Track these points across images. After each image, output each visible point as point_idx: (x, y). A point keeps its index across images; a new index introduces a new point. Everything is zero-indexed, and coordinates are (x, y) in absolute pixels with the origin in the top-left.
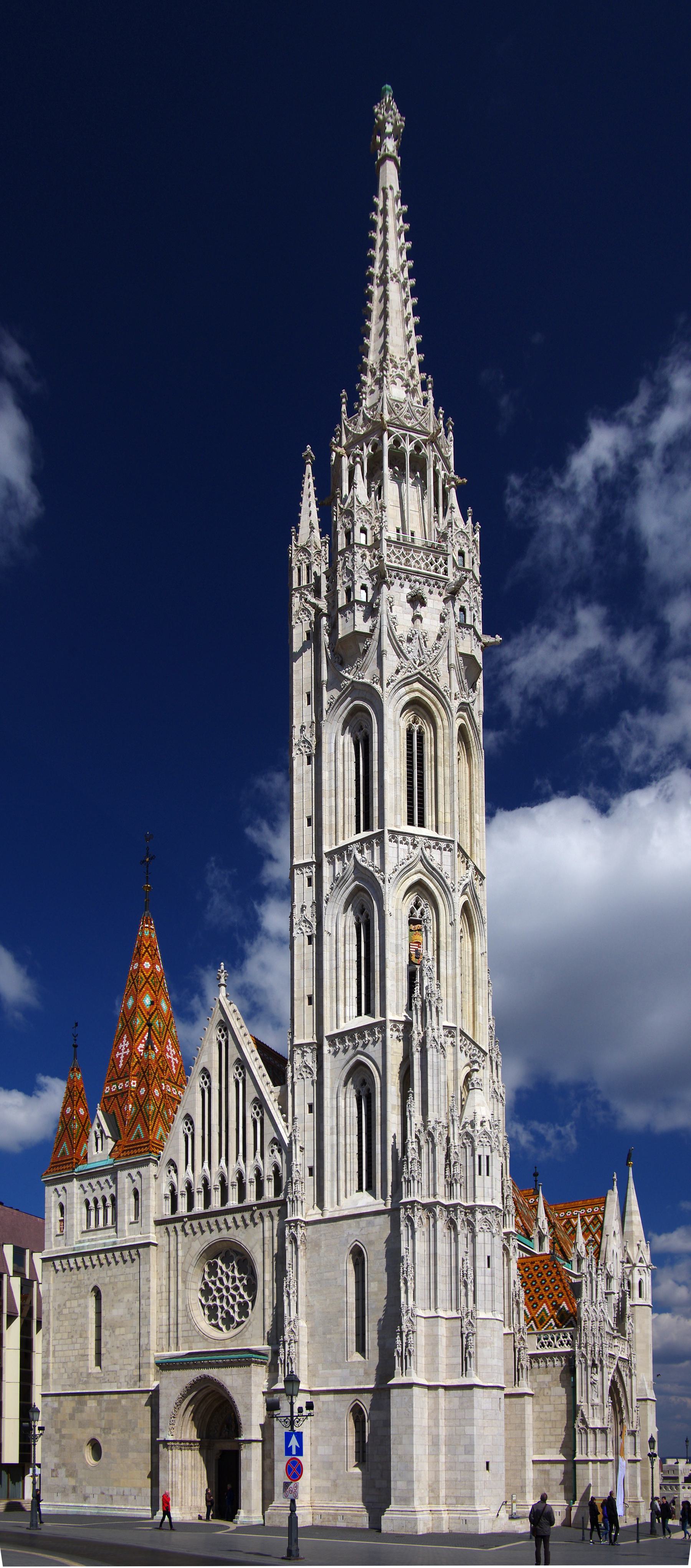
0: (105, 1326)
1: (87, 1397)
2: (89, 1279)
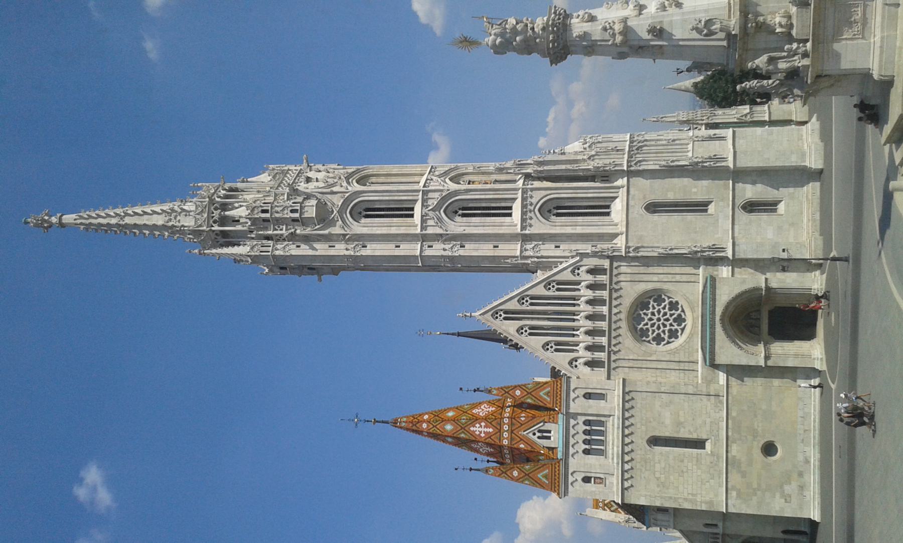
1: (729, 454)
2: (641, 449)
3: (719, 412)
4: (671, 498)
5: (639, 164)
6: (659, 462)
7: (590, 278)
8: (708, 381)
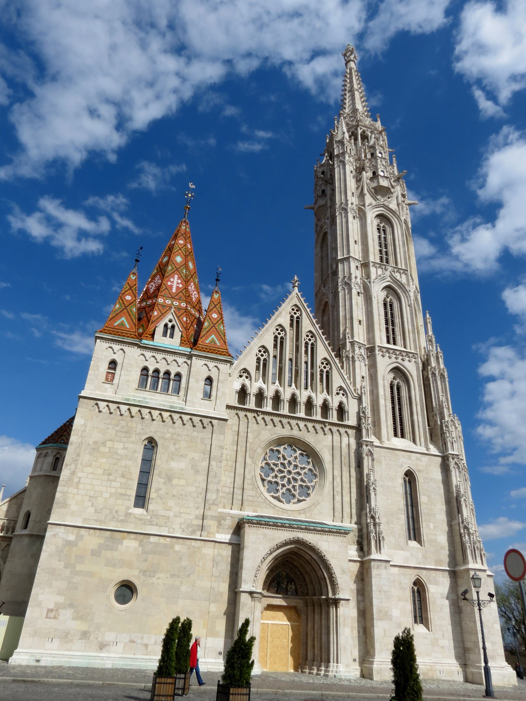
0: (159, 475)
2: (143, 429)
3: (180, 528)
4: (78, 455)
5: (456, 466)
6: (124, 448)
7: (334, 403)
8: (220, 519)
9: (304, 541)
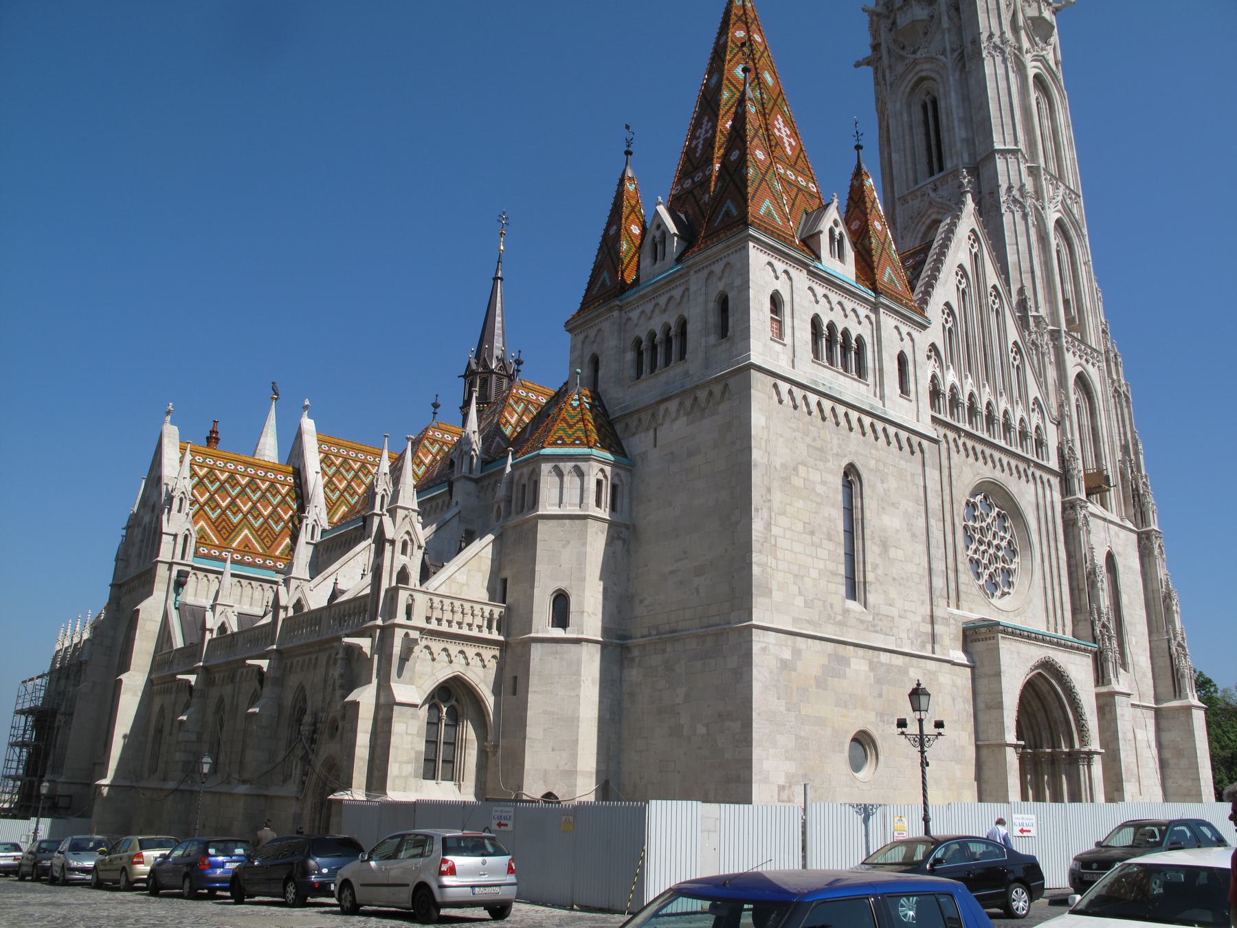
0: (873, 538)
3: (909, 638)
4: (769, 490)
6: (823, 483)
9: (1054, 663)
